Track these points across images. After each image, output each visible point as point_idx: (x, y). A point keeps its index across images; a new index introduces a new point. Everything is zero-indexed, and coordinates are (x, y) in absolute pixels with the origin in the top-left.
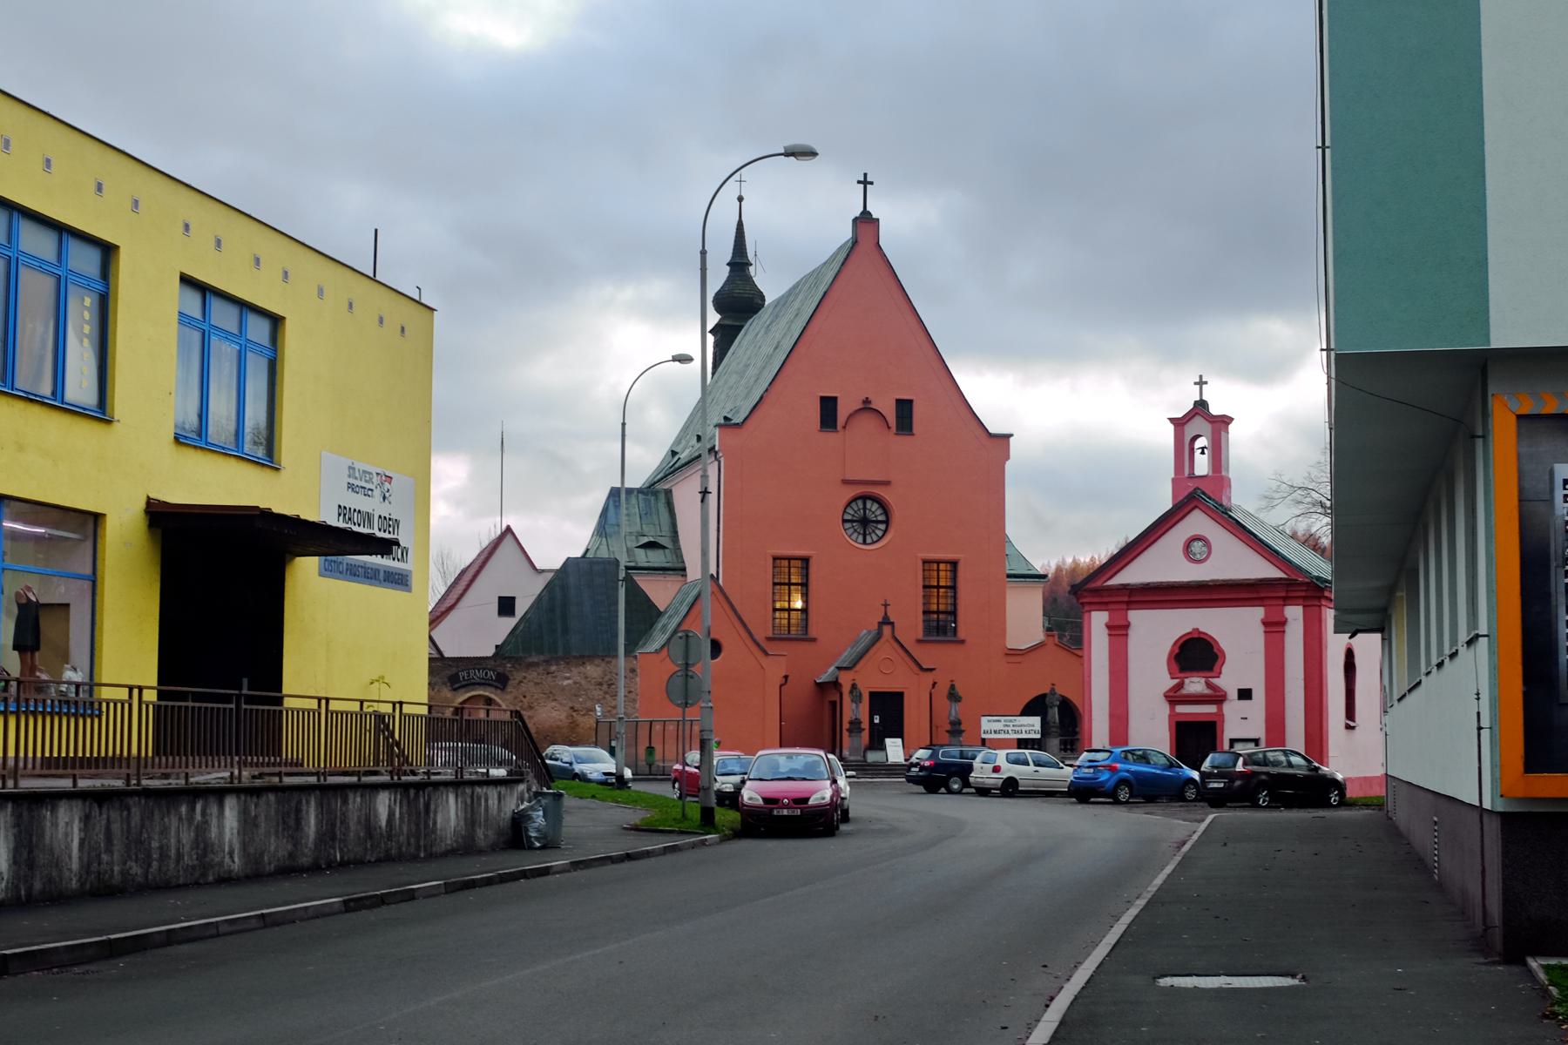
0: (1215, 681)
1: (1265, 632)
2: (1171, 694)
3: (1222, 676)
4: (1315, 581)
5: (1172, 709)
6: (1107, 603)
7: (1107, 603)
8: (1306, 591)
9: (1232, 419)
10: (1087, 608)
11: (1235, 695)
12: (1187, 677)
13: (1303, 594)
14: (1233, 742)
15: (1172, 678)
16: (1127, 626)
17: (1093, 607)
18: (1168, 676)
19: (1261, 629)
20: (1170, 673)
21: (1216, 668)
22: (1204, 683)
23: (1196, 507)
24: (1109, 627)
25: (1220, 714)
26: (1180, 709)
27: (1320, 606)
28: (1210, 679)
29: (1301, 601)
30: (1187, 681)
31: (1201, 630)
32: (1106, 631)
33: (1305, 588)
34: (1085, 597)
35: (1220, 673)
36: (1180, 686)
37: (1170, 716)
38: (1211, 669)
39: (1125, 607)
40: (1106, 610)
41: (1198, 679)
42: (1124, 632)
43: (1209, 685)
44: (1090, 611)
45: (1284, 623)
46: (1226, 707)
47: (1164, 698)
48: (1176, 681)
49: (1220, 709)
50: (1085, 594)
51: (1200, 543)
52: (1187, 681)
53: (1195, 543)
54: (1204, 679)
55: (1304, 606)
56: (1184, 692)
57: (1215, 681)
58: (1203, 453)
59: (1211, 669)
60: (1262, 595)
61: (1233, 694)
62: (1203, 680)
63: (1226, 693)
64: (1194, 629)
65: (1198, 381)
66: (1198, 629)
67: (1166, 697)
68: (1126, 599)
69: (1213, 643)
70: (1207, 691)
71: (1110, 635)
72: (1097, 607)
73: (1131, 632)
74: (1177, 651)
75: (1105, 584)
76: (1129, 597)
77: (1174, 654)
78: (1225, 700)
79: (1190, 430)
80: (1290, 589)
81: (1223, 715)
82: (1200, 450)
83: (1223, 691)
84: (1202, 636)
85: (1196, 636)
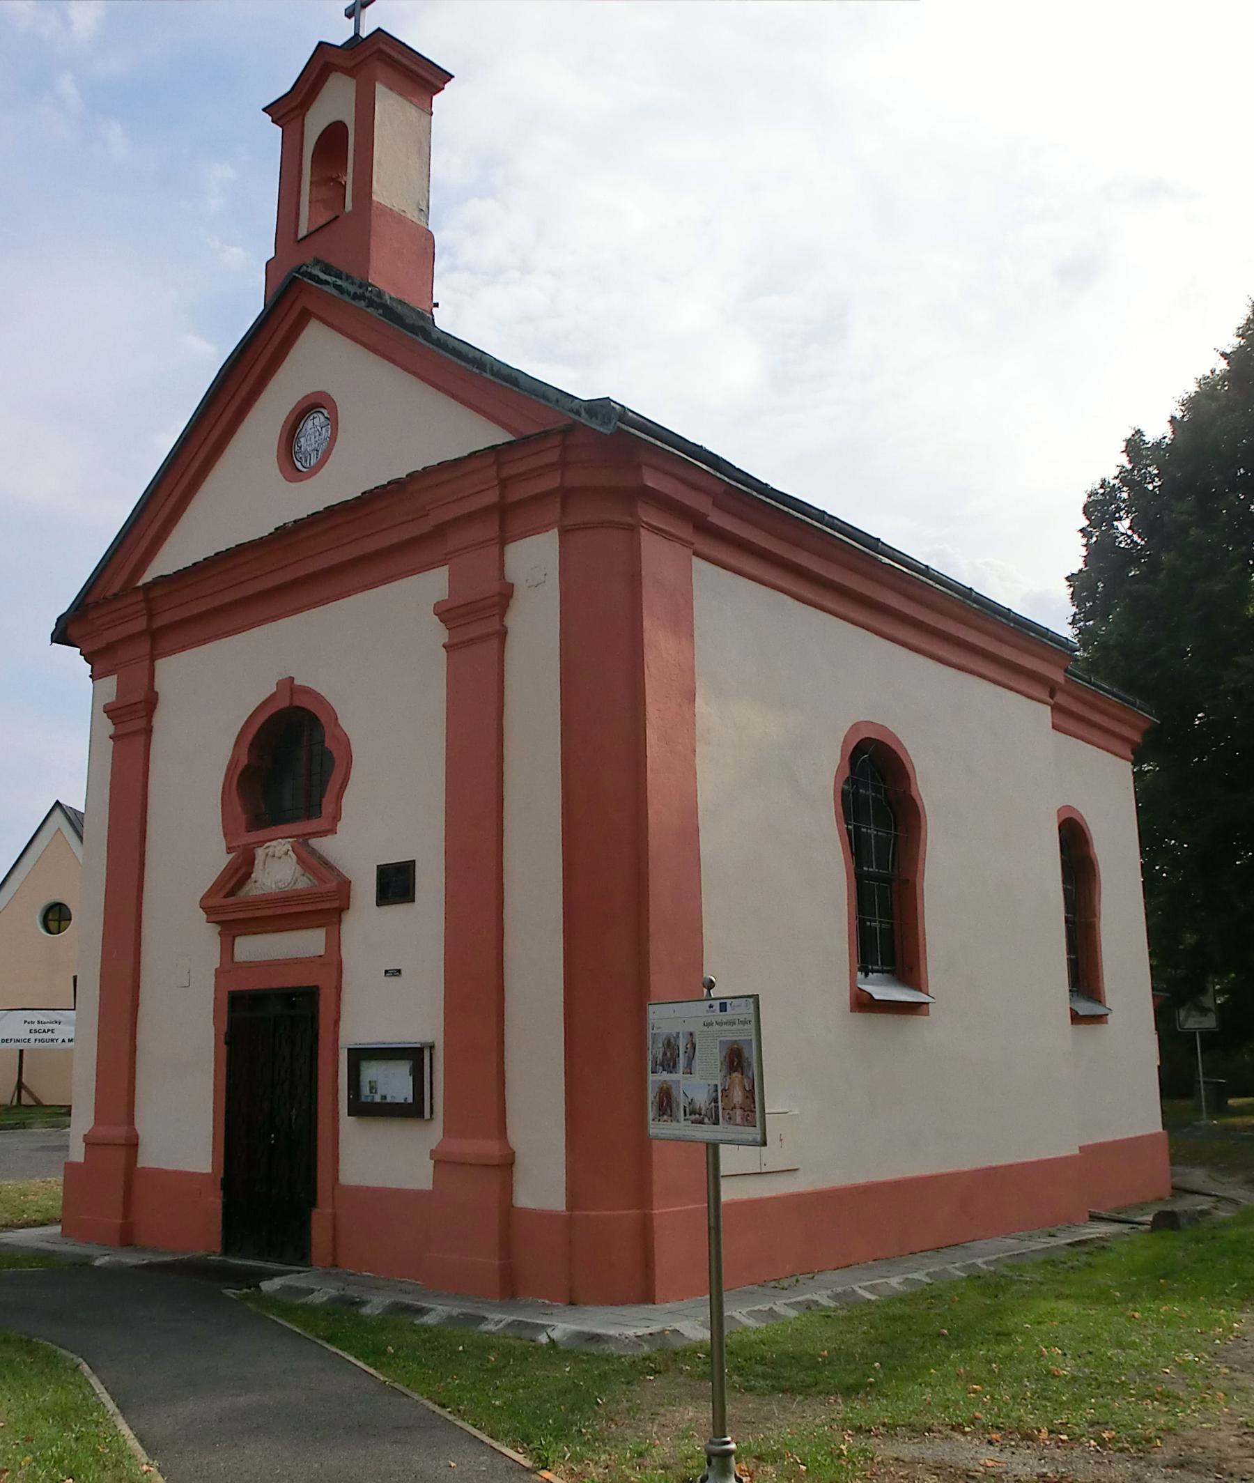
0: (324, 845)
2: (217, 901)
4: (584, 419)
8: (563, 464)
9: (453, 77)
12: (261, 843)
13: (551, 482)
14: (358, 1056)
25: (333, 961)
26: (251, 948)
27: (632, 529)
28: (315, 842)
31: (297, 682)
33: (553, 457)
35: (337, 817)
37: (218, 972)
38: (311, 808)
39: (144, 647)
42: (140, 724)
49: (334, 944)
52: (260, 853)
53: (310, 423)
55: (564, 533)
57: (324, 845)
61: (365, 887)
70: (303, 883)
74: (244, 761)
76: (151, 616)
77: (238, 772)
79: (316, 123)
80: (508, 471)
84: (300, 701)
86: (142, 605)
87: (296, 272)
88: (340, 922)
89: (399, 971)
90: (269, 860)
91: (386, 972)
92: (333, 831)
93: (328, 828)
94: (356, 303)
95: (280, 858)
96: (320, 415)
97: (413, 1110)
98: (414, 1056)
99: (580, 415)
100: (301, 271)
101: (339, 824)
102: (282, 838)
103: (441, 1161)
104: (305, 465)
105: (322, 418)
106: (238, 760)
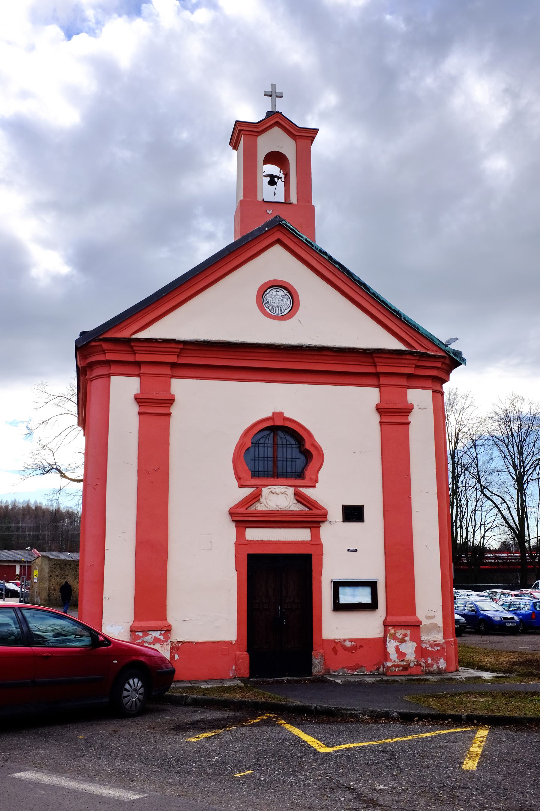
0: (308, 492)
1: (381, 423)
2: (242, 510)
3: (317, 485)
4: (452, 354)
5: (240, 534)
6: (138, 364)
7: (138, 364)
10: (98, 371)
11: (340, 517)
12: (266, 486)
14: (337, 585)
15: (241, 486)
16: (170, 401)
17: (114, 369)
18: (236, 483)
19: (376, 418)
20: (238, 478)
21: (308, 473)
22: (292, 496)
23: (279, 241)
24: (139, 400)
28: (301, 489)
29: (429, 383)
30: (265, 491)
31: (286, 415)
32: (135, 409)
33: (439, 365)
34: (104, 352)
35: (316, 481)
36: (256, 497)
39: (167, 371)
40: (138, 376)
41: (282, 489)
43: (300, 498)
44: (109, 376)
45: (408, 410)
46: (325, 531)
47: (228, 518)
48: (247, 491)
49: (316, 536)
50: (105, 346)
51: (281, 293)
52: (265, 491)
53: (273, 292)
54: (291, 491)
55: (434, 391)
56: (259, 507)
58: (272, 182)
59: (300, 475)
60: (380, 369)
62: (291, 491)
63: (327, 512)
64: (274, 413)
65: (269, 89)
66: (281, 414)
67: (232, 513)
68: (173, 359)
69: (304, 435)
71: (139, 413)
72: (121, 369)
73: (174, 410)
75: (134, 336)
76: (178, 356)
78: (324, 521)
81: (320, 545)
82: (268, 179)
83: (324, 509)
85: (279, 423)
86: (178, 350)
87: (281, 222)
88: (320, 527)
89: (356, 550)
90: (271, 494)
91: (349, 550)
92: (314, 487)
93: (313, 485)
94: (322, 255)
95: (278, 494)
96: (281, 291)
97: (372, 606)
98: (373, 585)
99: (450, 353)
100: (283, 222)
101: (317, 484)
102: (281, 485)
103: (386, 625)
104: (272, 311)
105: (283, 294)
106: (245, 443)
